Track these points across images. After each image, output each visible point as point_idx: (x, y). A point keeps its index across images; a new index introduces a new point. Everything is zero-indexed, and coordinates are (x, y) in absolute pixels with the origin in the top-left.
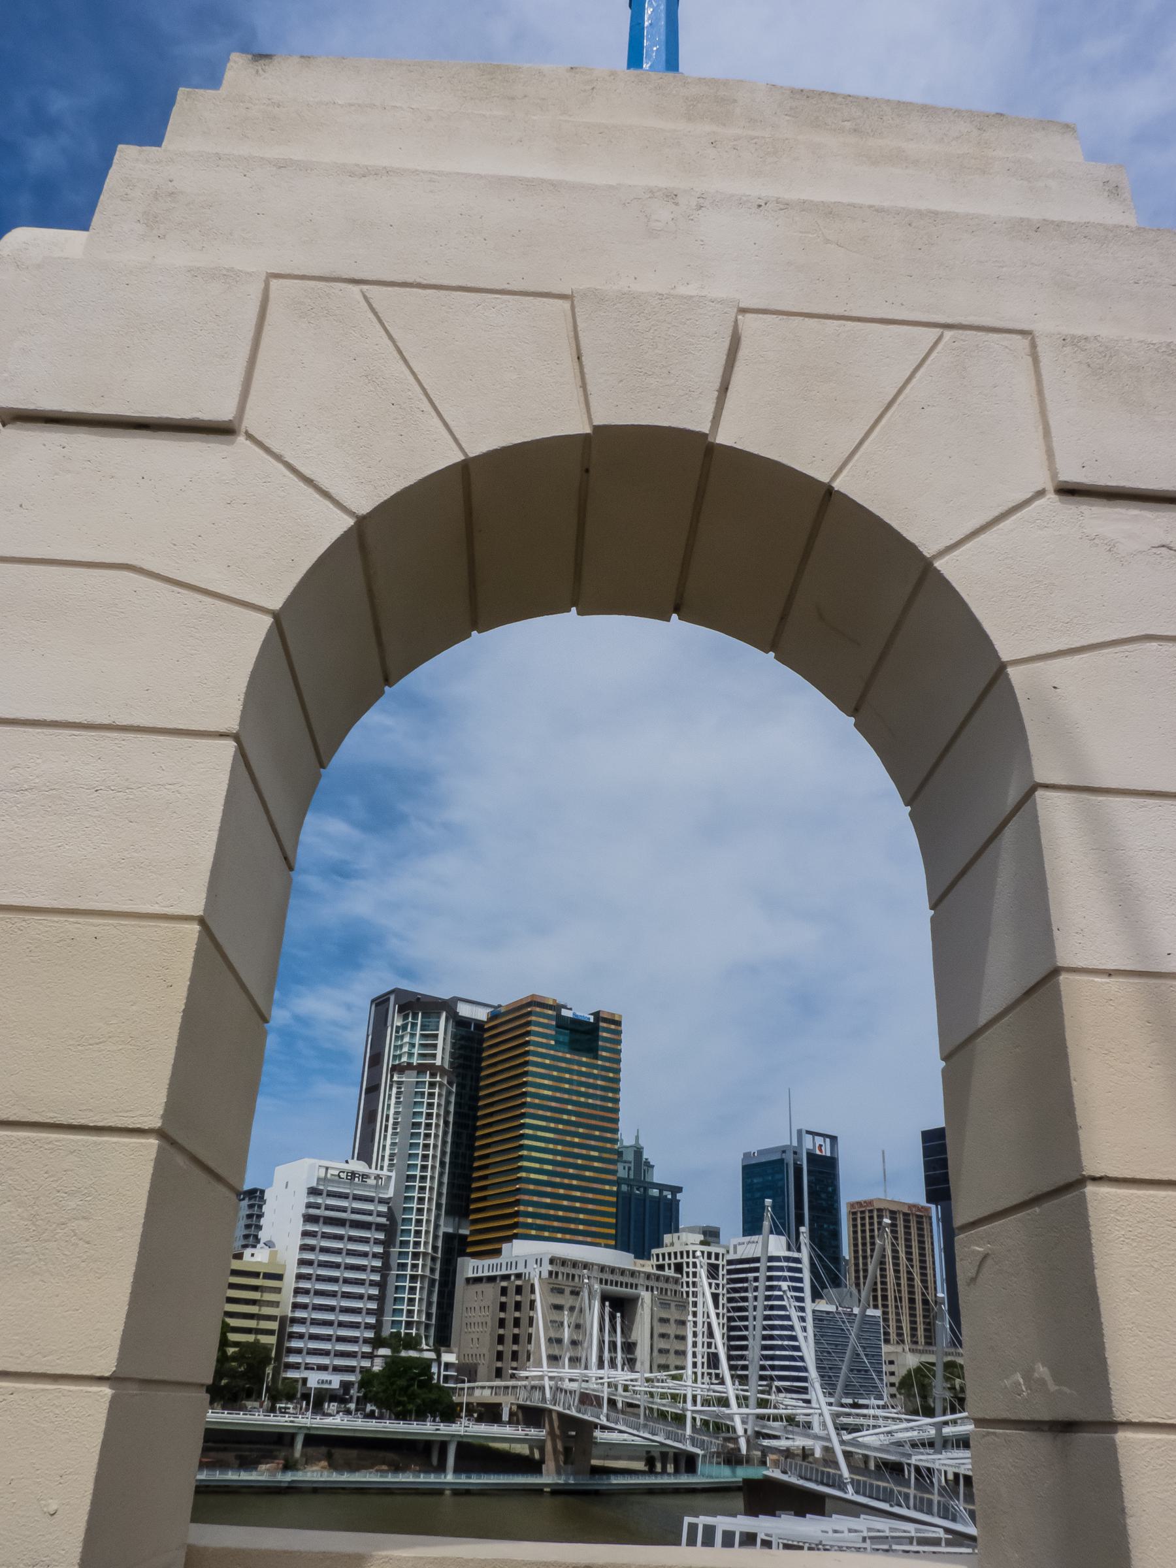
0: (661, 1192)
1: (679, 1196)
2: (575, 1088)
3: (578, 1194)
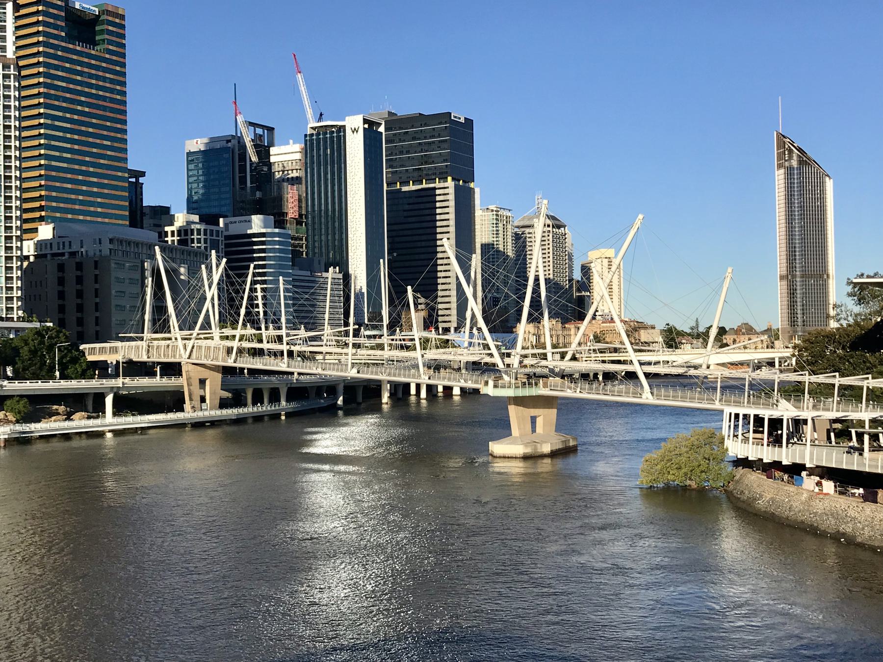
1: (141, 180)
3: (95, 180)
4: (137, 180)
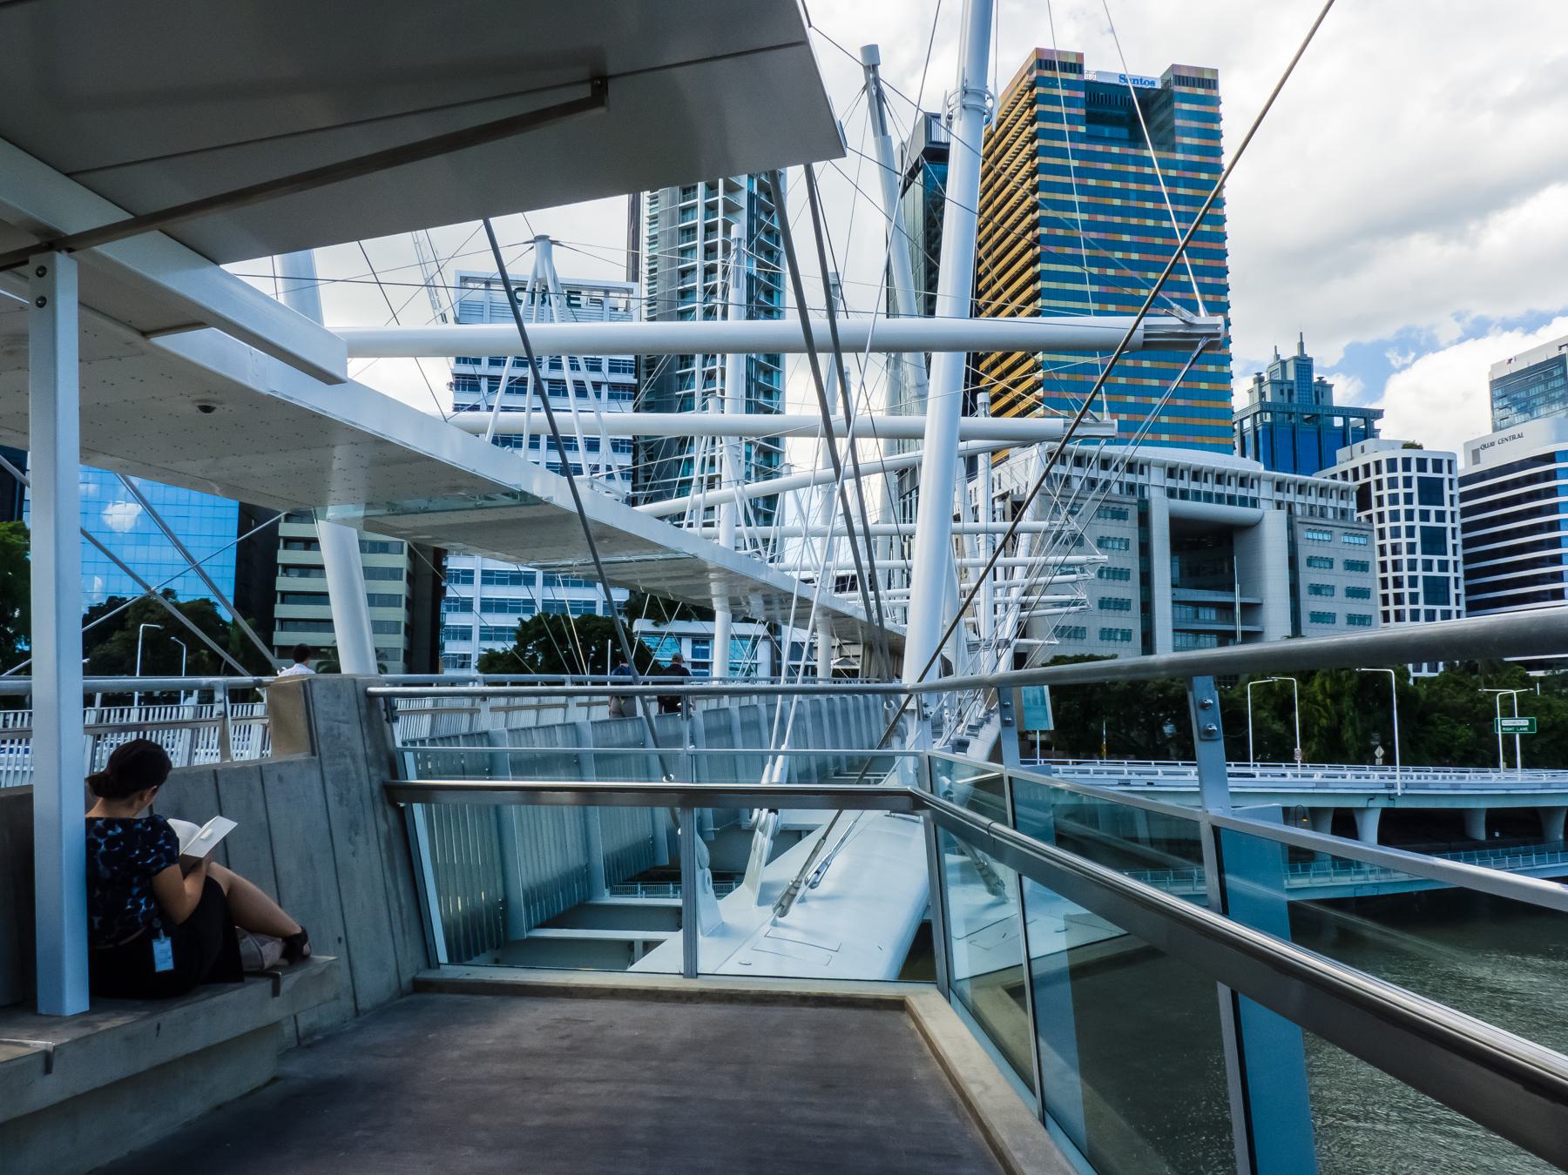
1: (1377, 424)
2: (1133, 203)
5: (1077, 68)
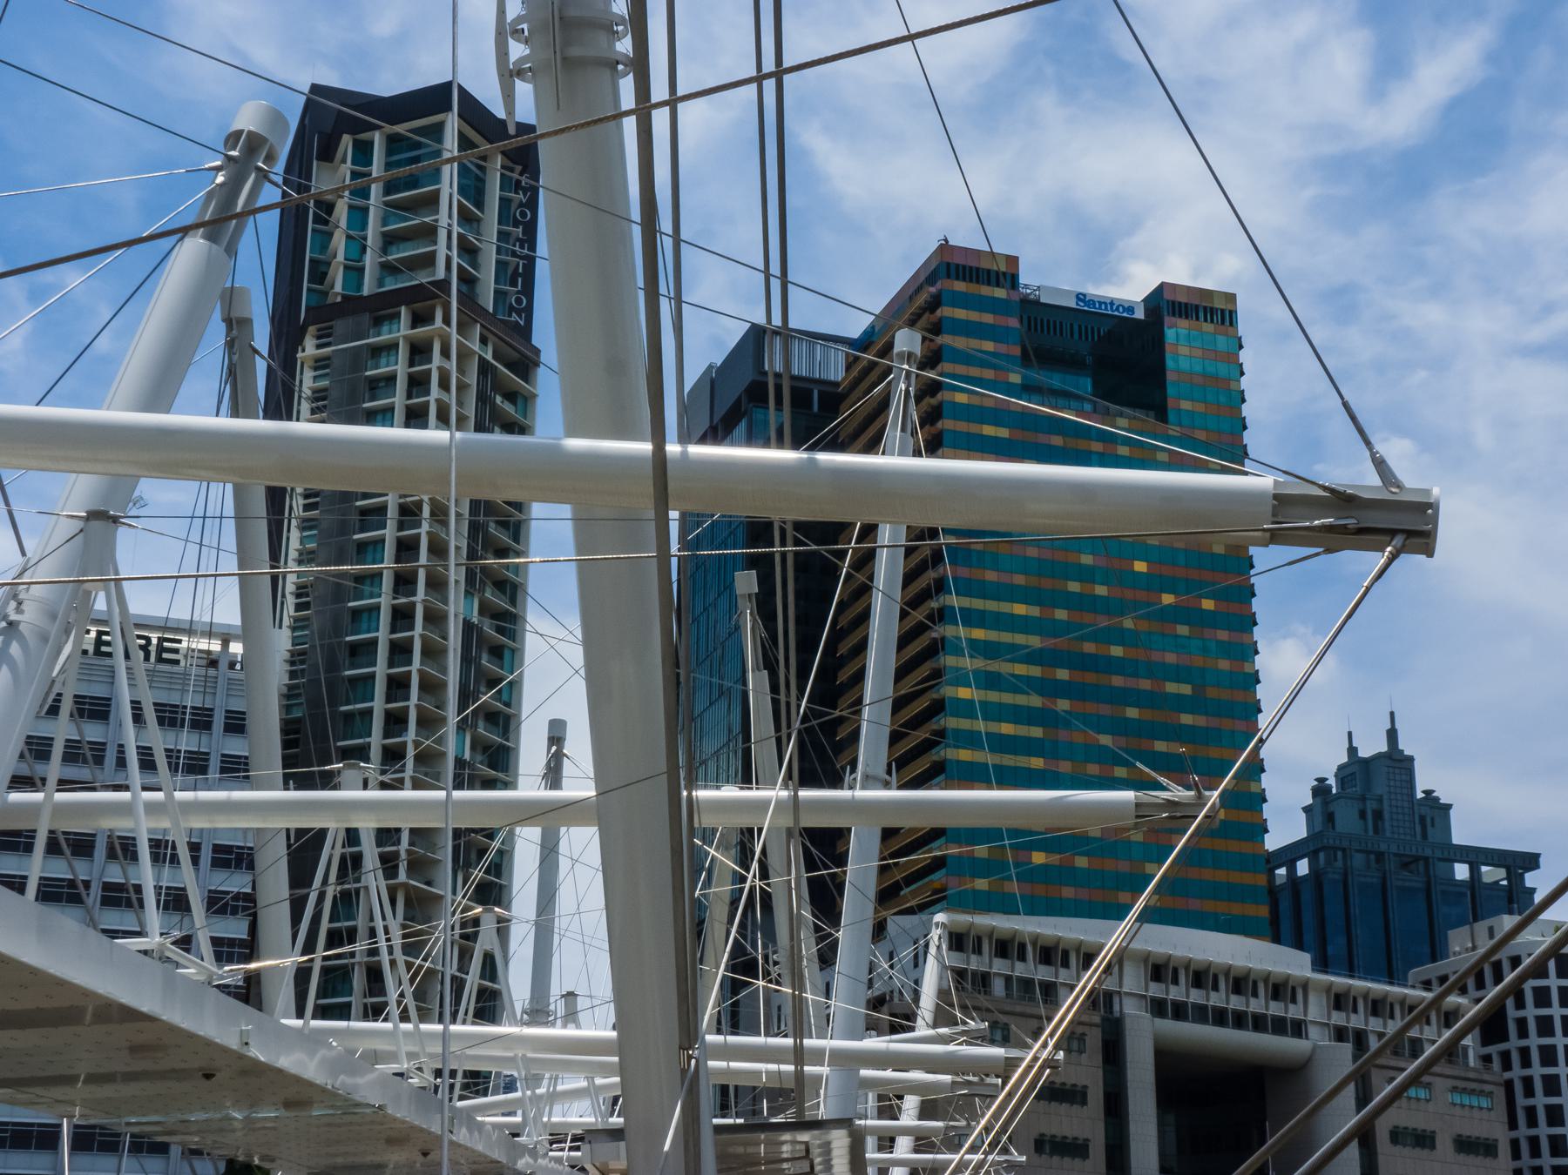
0: (1474, 871)
1: (1530, 879)
4: (1515, 878)
5: (1012, 280)
